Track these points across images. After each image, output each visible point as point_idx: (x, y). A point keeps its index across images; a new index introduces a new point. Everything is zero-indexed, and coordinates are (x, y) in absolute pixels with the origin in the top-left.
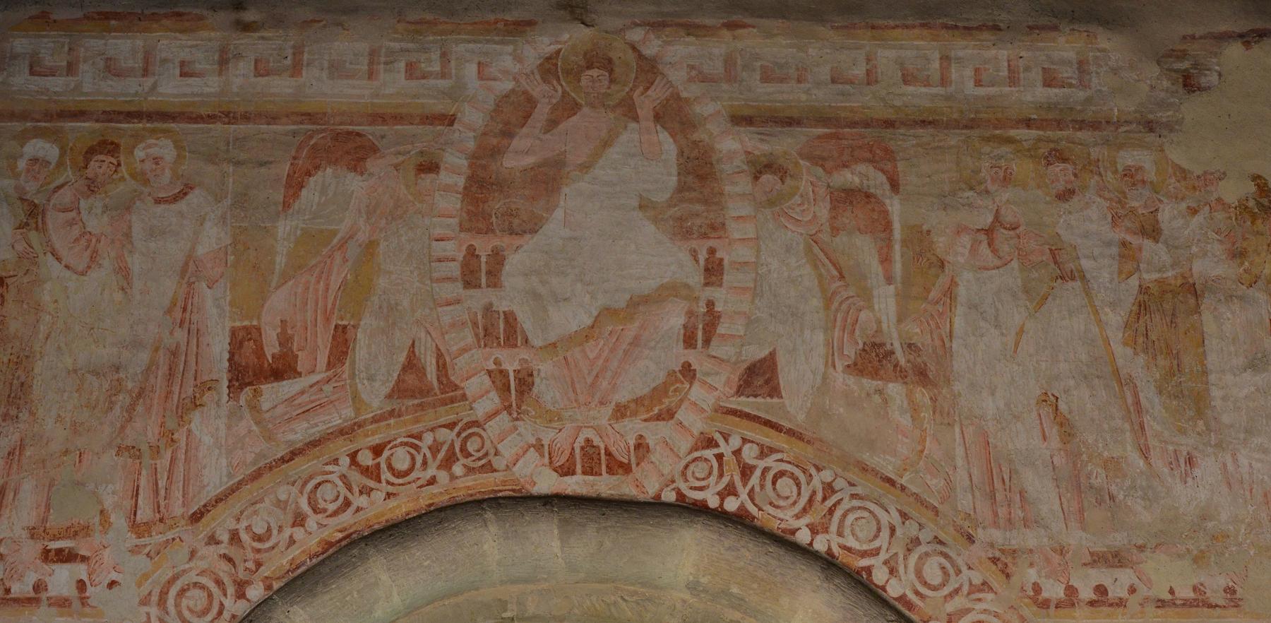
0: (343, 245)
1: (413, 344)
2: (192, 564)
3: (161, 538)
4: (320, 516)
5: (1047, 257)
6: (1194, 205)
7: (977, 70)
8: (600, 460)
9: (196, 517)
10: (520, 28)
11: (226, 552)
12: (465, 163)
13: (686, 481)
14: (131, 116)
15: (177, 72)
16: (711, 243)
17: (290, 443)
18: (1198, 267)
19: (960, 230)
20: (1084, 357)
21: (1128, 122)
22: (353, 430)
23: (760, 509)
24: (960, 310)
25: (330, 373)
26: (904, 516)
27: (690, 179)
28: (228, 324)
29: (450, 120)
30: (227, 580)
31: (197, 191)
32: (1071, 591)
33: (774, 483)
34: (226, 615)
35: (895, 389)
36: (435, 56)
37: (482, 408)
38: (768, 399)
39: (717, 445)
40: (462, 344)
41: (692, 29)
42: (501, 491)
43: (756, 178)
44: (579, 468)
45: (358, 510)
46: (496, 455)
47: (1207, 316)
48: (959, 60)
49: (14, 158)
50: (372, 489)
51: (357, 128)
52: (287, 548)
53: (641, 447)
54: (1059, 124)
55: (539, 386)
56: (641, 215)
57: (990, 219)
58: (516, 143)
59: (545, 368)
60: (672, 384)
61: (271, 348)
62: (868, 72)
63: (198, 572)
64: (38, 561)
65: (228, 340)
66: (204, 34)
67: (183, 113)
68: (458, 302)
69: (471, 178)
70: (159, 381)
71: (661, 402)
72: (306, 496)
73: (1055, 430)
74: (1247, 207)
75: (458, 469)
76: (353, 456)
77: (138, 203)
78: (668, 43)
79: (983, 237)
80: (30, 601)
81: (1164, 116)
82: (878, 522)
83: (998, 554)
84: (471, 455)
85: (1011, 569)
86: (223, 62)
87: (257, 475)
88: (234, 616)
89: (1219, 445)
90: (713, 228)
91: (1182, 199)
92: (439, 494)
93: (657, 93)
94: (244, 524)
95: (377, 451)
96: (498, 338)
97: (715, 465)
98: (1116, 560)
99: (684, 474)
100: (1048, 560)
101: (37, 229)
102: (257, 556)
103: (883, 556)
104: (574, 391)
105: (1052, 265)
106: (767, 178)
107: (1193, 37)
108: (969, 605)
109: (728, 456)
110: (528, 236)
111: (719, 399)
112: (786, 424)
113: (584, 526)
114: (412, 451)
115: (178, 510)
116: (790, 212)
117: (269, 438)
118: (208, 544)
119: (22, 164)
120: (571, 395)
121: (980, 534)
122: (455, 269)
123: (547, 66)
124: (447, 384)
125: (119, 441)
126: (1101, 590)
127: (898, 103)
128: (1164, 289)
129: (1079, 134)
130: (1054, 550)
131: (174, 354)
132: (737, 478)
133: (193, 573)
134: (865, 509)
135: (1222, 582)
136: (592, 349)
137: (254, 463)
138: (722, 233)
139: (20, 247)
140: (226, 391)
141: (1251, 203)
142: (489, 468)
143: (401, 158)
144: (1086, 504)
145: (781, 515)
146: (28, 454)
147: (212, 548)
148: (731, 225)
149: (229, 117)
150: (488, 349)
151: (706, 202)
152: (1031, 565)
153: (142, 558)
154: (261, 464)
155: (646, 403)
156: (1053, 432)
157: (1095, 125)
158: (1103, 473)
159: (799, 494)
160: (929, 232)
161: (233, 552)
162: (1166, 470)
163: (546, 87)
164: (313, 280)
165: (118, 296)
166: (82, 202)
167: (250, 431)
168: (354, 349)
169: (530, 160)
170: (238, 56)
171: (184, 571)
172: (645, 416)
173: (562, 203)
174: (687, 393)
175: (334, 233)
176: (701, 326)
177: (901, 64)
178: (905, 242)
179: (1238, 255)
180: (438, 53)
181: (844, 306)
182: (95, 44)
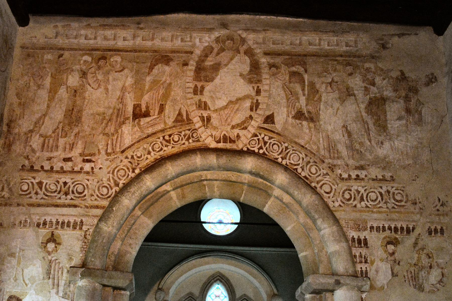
1: (180, 109)
2: (121, 164)
3: (113, 157)
4: (155, 152)
5: (345, 90)
6: (384, 77)
7: (328, 42)
9: (123, 152)
10: (211, 30)
12: (195, 64)
13: (250, 145)
14: (110, 50)
15: (122, 39)
16: (258, 85)
17: (148, 133)
18: (385, 93)
20: (354, 116)
21: (368, 56)
23: (269, 153)
25: (158, 116)
26: (306, 155)
28: (133, 103)
29: (192, 53)
30: (130, 168)
31: (126, 69)
32: (350, 176)
34: (130, 177)
35: (305, 123)
36: (189, 36)
37: (197, 126)
38: (272, 125)
39: (258, 136)
40: (193, 109)
41: (254, 31)
43: (270, 68)
45: (165, 151)
48: (324, 40)
49: (80, 61)
50: (168, 146)
53: (238, 136)
54: (349, 56)
55: (212, 120)
56: (240, 78)
57: (330, 80)
59: (214, 115)
61: (144, 109)
62: (300, 42)
66: (129, 30)
67: (123, 50)
68: (192, 98)
69: (197, 67)
70: (114, 117)
71: (243, 125)
72: (151, 146)
73: (346, 135)
74: (398, 78)
75: (191, 141)
76: (164, 137)
77: (111, 72)
80: (79, 172)
81: (377, 55)
82: (299, 157)
83: (330, 166)
85: (334, 170)
86: (134, 37)
87: (139, 141)
91: (382, 76)
93: (245, 47)
94: (135, 153)
95: (170, 136)
100: (344, 168)
101: (85, 78)
103: (300, 166)
107: (385, 35)
109: (261, 139)
110: (210, 83)
112: (276, 131)
113: (222, 156)
115: (118, 150)
116: (279, 78)
117: (142, 132)
119: (82, 62)
121: (326, 161)
122: (191, 90)
124: (188, 119)
125: (104, 132)
126: (357, 176)
129: (354, 59)
130: (345, 165)
131: (119, 110)
132: (263, 145)
133: (121, 166)
134: (296, 153)
135: (390, 174)
136: (226, 111)
137: (138, 138)
138: (260, 82)
139: (81, 82)
140: (131, 120)
142: (198, 141)
143: (179, 62)
145: (274, 154)
146: (80, 134)
147: (126, 160)
148: (264, 80)
149: (135, 51)
151: (257, 75)
152: (339, 169)
153: (108, 162)
154: (140, 138)
155: (240, 125)
157: (359, 57)
159: (279, 149)
161: (132, 161)
162: (376, 145)
163: (216, 45)
164: (155, 92)
165: (105, 95)
166: (97, 72)
169: (212, 63)
170: (138, 36)
173: (220, 74)
174: (250, 123)
175: (161, 81)
179: (396, 90)
182: (102, 32)
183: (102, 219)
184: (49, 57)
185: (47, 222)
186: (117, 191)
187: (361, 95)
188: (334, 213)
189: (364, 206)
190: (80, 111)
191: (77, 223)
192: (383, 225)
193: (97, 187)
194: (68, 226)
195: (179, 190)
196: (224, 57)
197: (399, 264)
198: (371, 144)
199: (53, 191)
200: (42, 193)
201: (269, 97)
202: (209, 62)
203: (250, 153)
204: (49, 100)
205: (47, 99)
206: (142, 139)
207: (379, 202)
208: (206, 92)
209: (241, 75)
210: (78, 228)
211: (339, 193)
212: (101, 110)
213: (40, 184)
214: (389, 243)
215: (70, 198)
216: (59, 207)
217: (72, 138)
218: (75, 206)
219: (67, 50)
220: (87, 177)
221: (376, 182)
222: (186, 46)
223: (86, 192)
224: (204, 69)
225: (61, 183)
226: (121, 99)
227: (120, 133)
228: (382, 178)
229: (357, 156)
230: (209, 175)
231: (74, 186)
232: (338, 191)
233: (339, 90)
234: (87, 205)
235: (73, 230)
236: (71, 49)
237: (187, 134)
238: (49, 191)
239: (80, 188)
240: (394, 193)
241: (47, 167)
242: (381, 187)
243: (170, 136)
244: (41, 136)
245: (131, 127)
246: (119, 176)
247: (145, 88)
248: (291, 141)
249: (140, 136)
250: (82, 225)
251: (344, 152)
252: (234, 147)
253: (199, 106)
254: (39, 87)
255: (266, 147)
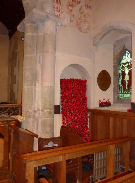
197: (73, 16)
214: (70, 5)
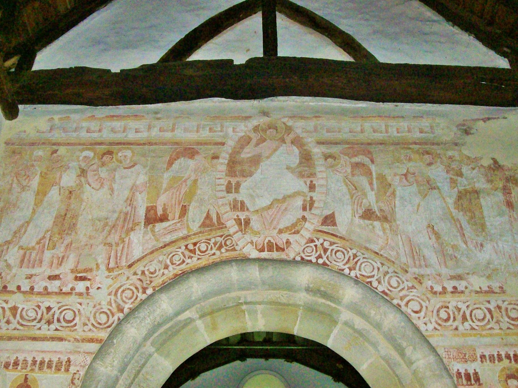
0: (185, 181)
1: (209, 211)
2: (127, 282)
3: (116, 273)
4: (174, 266)
6: (473, 167)
7: (397, 129)
8: (273, 247)
9: (130, 266)
11: (140, 278)
12: (228, 156)
13: (304, 253)
15: (134, 131)
16: (311, 179)
18: (477, 185)
19: (395, 175)
22: (186, 238)
23: (331, 263)
24: (397, 199)
25: (180, 220)
26: (382, 264)
27: (303, 160)
29: (223, 144)
31: (138, 165)
32: (444, 288)
33: (335, 253)
34: (139, 299)
35: (377, 224)
36: (219, 126)
38: (332, 227)
39: (315, 242)
40: (226, 211)
42: (238, 257)
43: (326, 160)
44: (266, 249)
45: (187, 264)
46: (237, 245)
47: (482, 201)
48: (392, 126)
49: (78, 157)
50: (192, 257)
51: (192, 147)
52: (161, 277)
53: (288, 242)
54: (426, 144)
55: (252, 223)
56: (287, 171)
57: (405, 171)
58: (246, 150)
60: (299, 223)
61: (160, 212)
62: (361, 130)
63: (129, 284)
64: (73, 281)
65: (145, 210)
68: (224, 197)
69: (229, 161)
70: (120, 223)
71: (295, 228)
73: (433, 236)
74: (491, 167)
75: (223, 250)
78: (295, 122)
79: (404, 177)
82: (373, 266)
83: (417, 276)
84: (228, 246)
85: (422, 281)
87: (152, 252)
88: (141, 300)
89: (491, 240)
90: (311, 174)
92: (216, 258)
93: (292, 136)
94: (147, 268)
95: (195, 244)
96: (238, 209)
97: (314, 248)
98: (459, 278)
99: (303, 251)
101: (84, 177)
102: (151, 279)
103: (376, 277)
104: (264, 225)
105: (427, 185)
106: (328, 160)
108: (408, 294)
109: (319, 245)
110: (248, 178)
111: (315, 227)
113: (267, 267)
114: (207, 244)
115: (124, 263)
116: (338, 170)
117: (157, 240)
118: (134, 275)
119: (81, 158)
120: (264, 227)
122: (224, 188)
123: (256, 128)
126: (455, 288)
127: (372, 138)
128: (466, 191)
130: (437, 275)
132: (322, 253)
134: (368, 262)
135: (498, 284)
136: (270, 212)
137: (151, 249)
138: (315, 176)
139: (78, 182)
141: (492, 166)
142: (234, 250)
143: (207, 155)
144: (447, 260)
145: (338, 264)
146: (73, 245)
147: (135, 276)
149: (150, 144)
150: (234, 212)
151: (309, 167)
152: (429, 280)
154: (154, 249)
156: (433, 237)
157: (438, 144)
158: (451, 249)
159: (345, 257)
160: (385, 175)
161: (142, 278)
162: (474, 248)
163: (254, 134)
164: (175, 191)
165: (109, 197)
166: (100, 169)
167: (151, 238)
168: (188, 213)
169: (249, 155)
171: (125, 284)
172: (290, 233)
173: (260, 168)
175: (183, 177)
176: (308, 204)
177: (372, 127)
178: (377, 178)
180: (220, 125)
181: (357, 198)
182: (109, 124)
183: (98, 355)
184: (39, 153)
185: (19, 361)
186: (121, 318)
187: (446, 188)
188: (427, 338)
189: (469, 327)
190: (75, 217)
191: (62, 363)
192: (498, 352)
193: (93, 312)
194: (49, 367)
195: (208, 318)
196: (265, 148)
198: (468, 247)
199: (31, 319)
200: (16, 322)
201: (327, 194)
202: (247, 153)
203: (305, 262)
204: (35, 204)
205: (33, 203)
206: (157, 250)
207: (489, 320)
208: (242, 190)
209: (288, 168)
210: (63, 369)
211: (433, 311)
212: (104, 214)
213: (14, 310)
215: (55, 328)
216: (37, 341)
217: (62, 249)
218: (61, 339)
219: (63, 146)
220: (80, 300)
221: (481, 294)
222: (217, 137)
223: (77, 320)
224: (240, 163)
225: (43, 308)
226: (130, 201)
227: (127, 242)
228: (487, 289)
229: (450, 263)
230: (249, 295)
231: (61, 312)
232: (430, 309)
233: (417, 182)
234: (77, 337)
235: (55, 373)
236: (68, 143)
237: (218, 242)
238: (25, 319)
239: (69, 316)
240: (507, 309)
241: (25, 288)
242: (489, 302)
243: (195, 244)
244: (21, 248)
245: (142, 235)
246: (124, 299)
247: (162, 186)
248: (361, 247)
249: (154, 246)
250: (69, 365)
251: (433, 258)
252: (282, 256)
253: (234, 206)
254: (23, 188)
255: (327, 255)
